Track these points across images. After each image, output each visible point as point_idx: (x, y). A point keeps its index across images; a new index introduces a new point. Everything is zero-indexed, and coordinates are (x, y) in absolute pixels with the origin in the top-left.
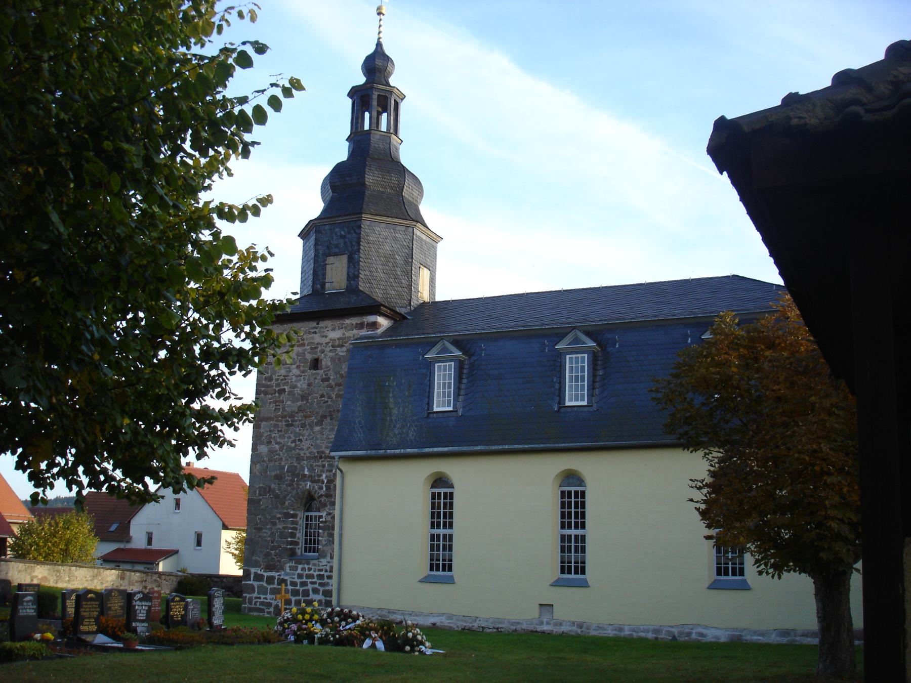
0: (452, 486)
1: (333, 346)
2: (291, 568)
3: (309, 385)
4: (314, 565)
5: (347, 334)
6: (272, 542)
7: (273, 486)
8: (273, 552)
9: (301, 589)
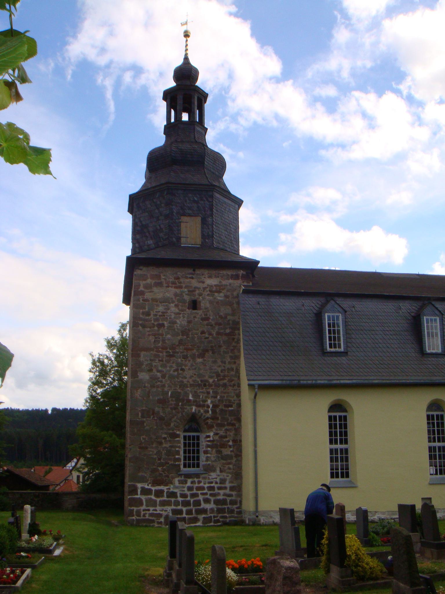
0: (345, 411)
1: (210, 291)
2: (180, 482)
3: (189, 322)
4: (204, 478)
5: (224, 283)
6: (159, 459)
7: (157, 409)
8: (160, 469)
9: (192, 500)
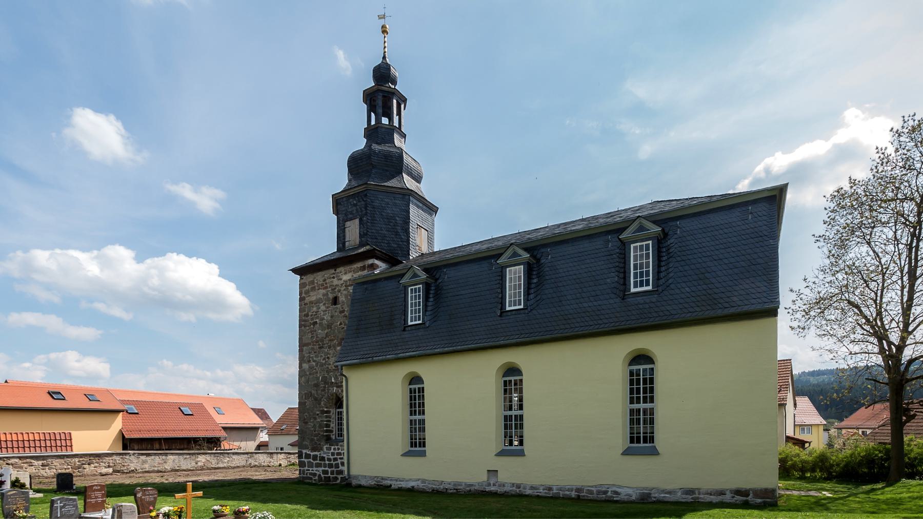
3: (332, 317)
